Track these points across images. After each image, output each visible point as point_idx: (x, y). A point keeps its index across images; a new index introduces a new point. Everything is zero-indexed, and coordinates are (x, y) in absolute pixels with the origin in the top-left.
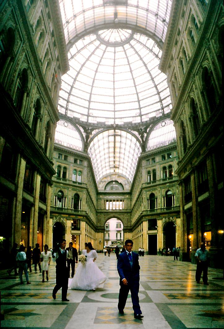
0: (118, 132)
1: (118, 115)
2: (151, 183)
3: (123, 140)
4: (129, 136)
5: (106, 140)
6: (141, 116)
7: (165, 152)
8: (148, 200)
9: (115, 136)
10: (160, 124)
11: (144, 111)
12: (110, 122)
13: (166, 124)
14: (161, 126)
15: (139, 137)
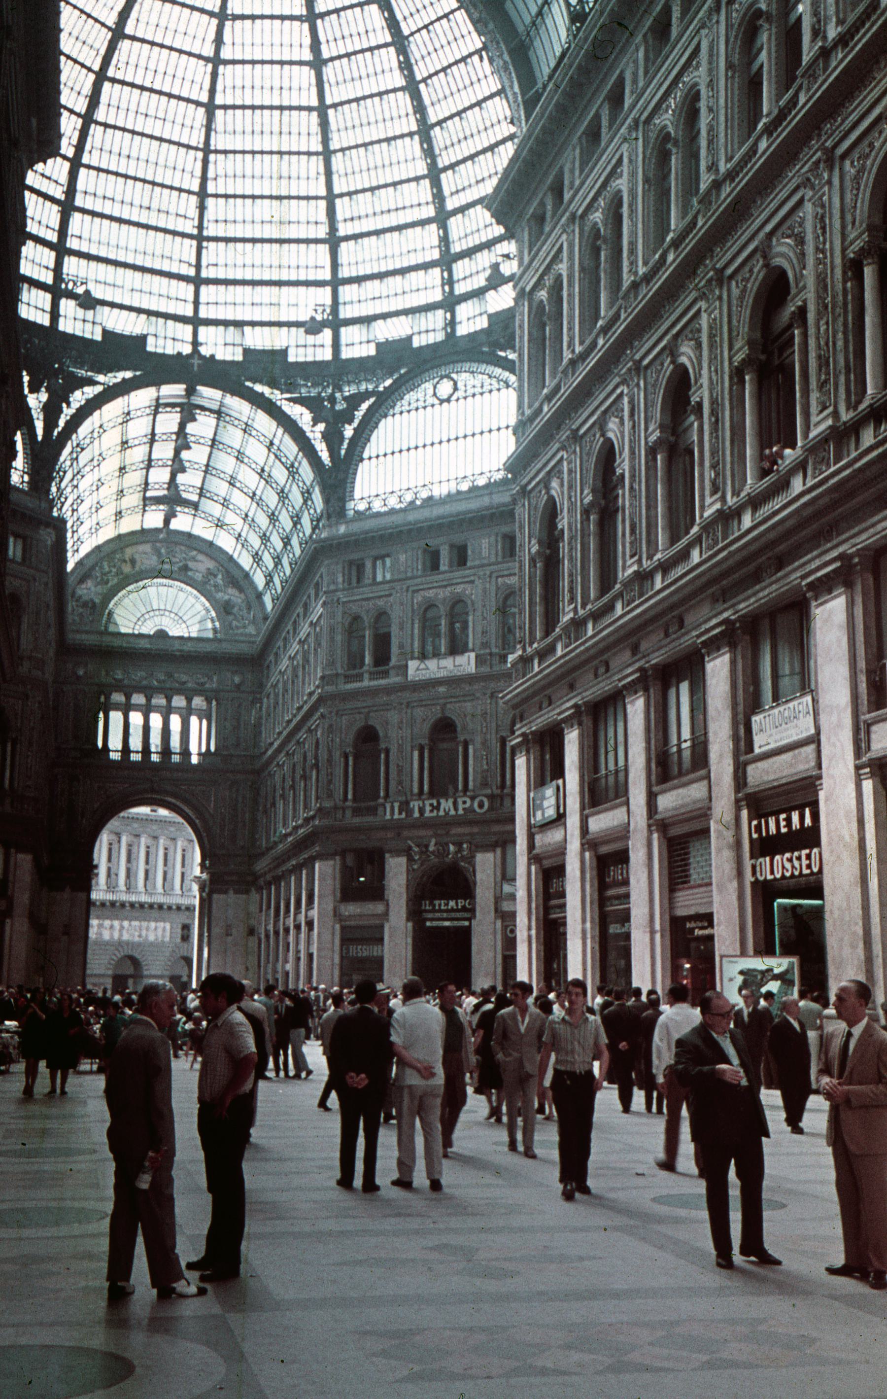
0: (209, 395)
1: (216, 302)
2: (366, 676)
3: (233, 436)
4: (264, 423)
5: (139, 428)
6: (336, 323)
7: (440, 534)
8: (346, 757)
9: (188, 411)
10: (428, 386)
11: (355, 301)
12: (169, 341)
13: (456, 389)
14: (431, 400)
15: (315, 433)
